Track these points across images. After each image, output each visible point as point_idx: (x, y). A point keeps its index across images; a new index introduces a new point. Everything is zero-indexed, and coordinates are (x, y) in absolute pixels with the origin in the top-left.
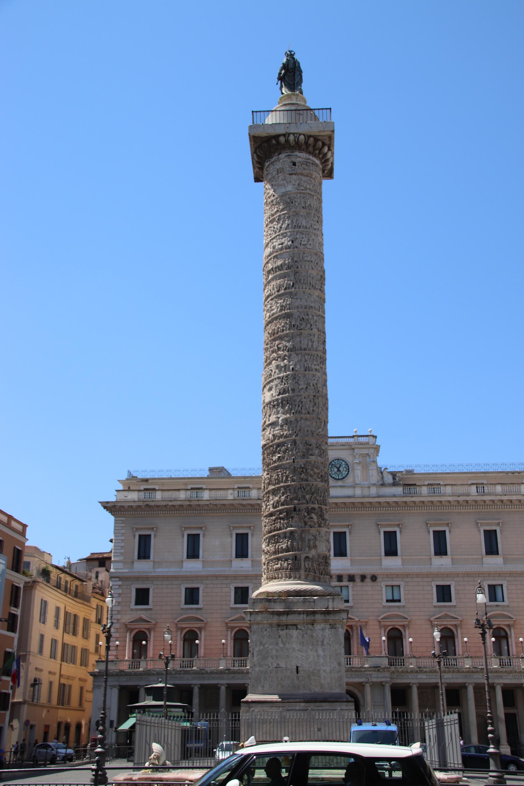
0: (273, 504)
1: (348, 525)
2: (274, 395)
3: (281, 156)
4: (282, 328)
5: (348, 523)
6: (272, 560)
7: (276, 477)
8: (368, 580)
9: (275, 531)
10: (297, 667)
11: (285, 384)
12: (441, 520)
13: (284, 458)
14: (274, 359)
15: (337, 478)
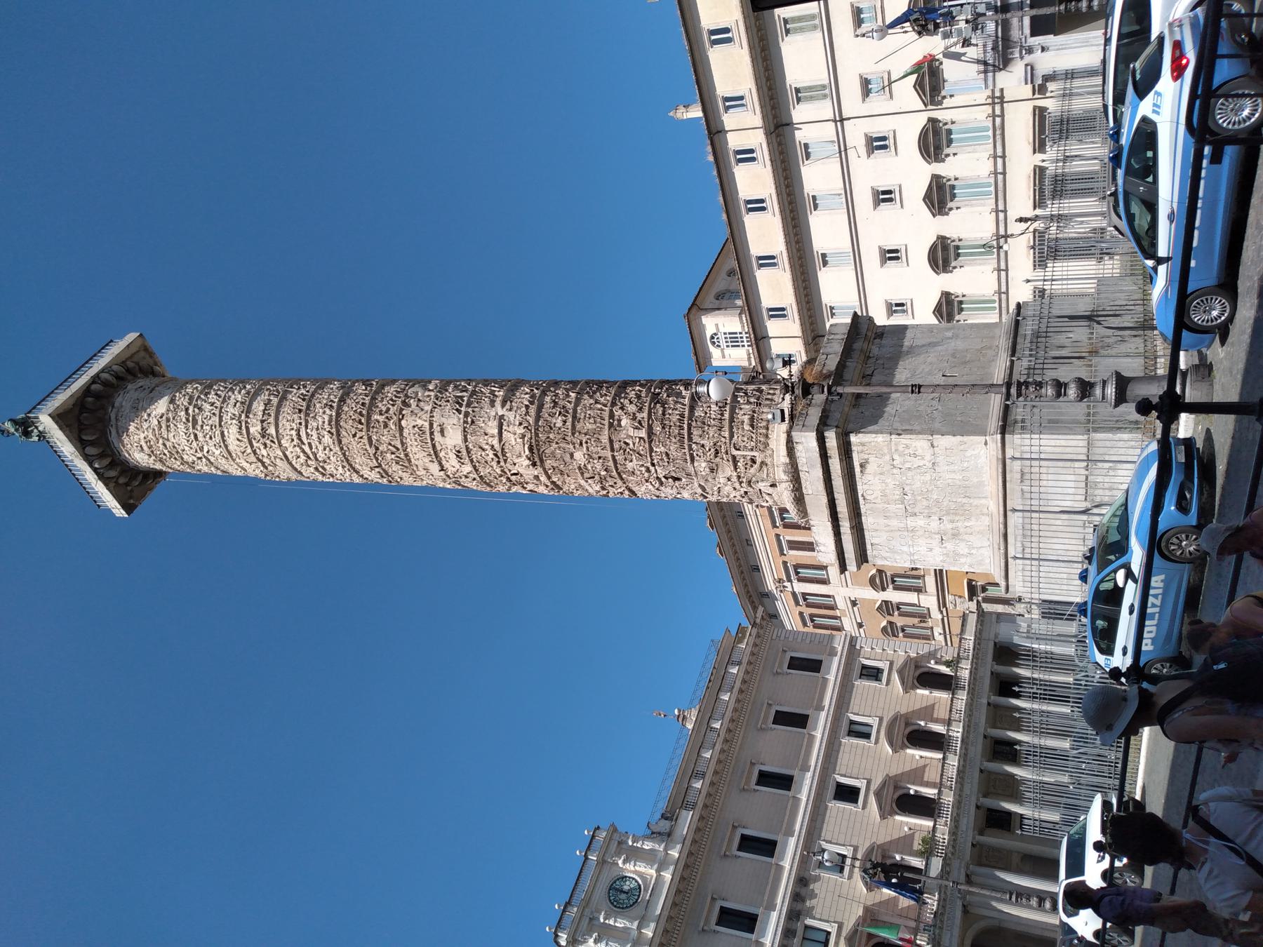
0: (636, 428)
1: (713, 899)
2: (455, 422)
3: (117, 404)
4: (359, 406)
5: (709, 898)
6: (732, 436)
7: (592, 419)
8: (803, 891)
9: (681, 428)
10: (943, 376)
11: (448, 401)
12: (743, 772)
13: (564, 407)
14: (400, 420)
15: (636, 897)
